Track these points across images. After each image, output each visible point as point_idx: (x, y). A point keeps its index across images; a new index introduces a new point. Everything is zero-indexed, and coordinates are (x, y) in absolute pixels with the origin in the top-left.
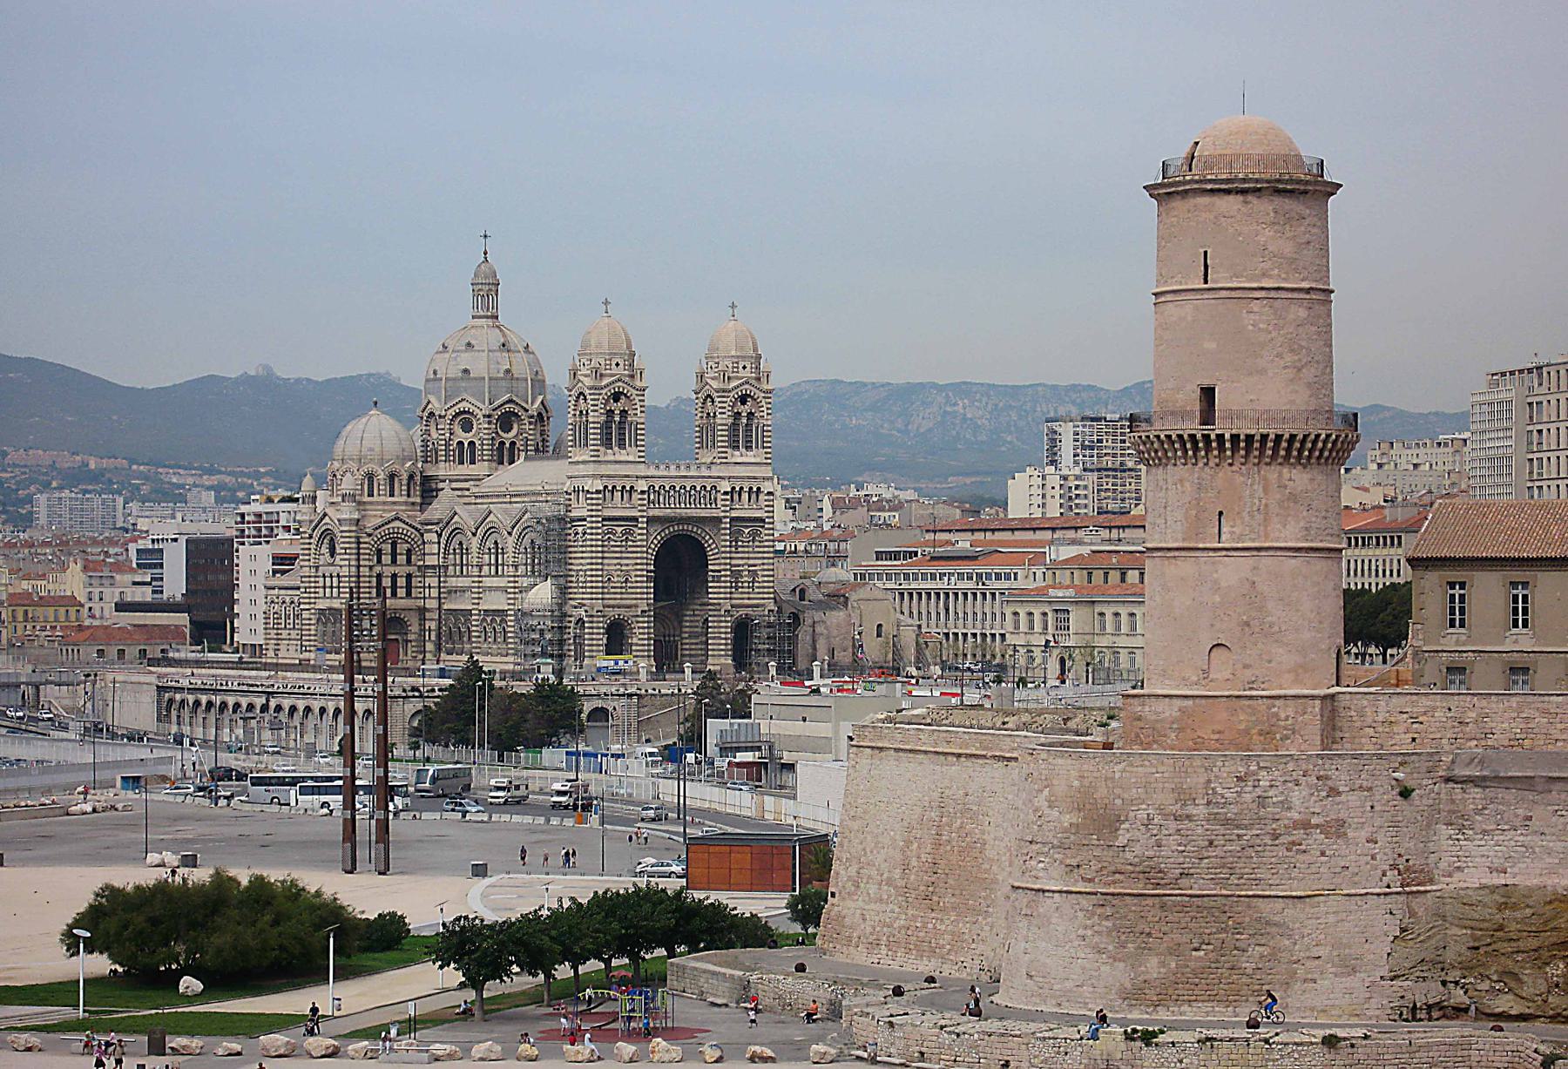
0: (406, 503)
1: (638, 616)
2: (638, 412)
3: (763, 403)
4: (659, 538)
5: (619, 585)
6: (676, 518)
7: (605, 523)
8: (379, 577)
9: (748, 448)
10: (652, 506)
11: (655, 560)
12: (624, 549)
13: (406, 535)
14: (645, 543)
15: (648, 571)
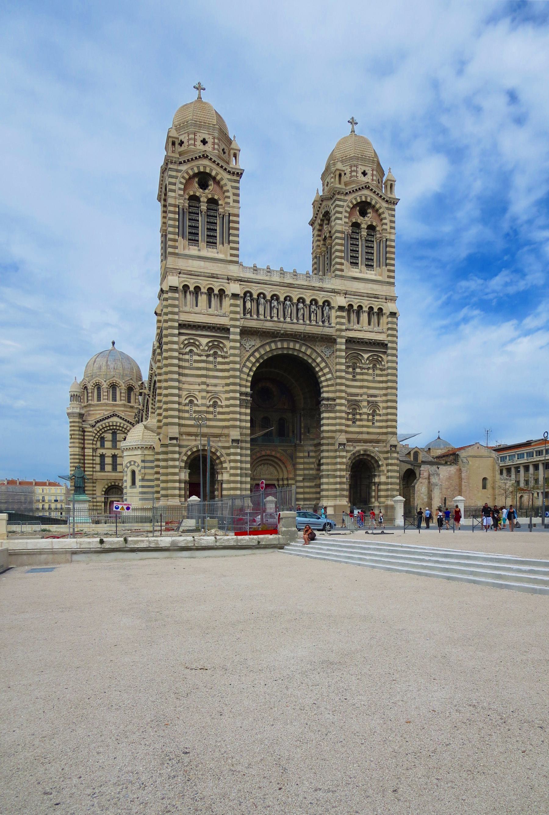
0: (124, 405)
1: (229, 448)
2: (230, 201)
3: (386, 215)
4: (257, 355)
5: (204, 409)
6: (278, 333)
7: (183, 331)
8: (102, 456)
9: (369, 266)
10: (248, 316)
11: (252, 382)
12: (211, 366)
13: (126, 429)
14: (238, 359)
15: (241, 394)
